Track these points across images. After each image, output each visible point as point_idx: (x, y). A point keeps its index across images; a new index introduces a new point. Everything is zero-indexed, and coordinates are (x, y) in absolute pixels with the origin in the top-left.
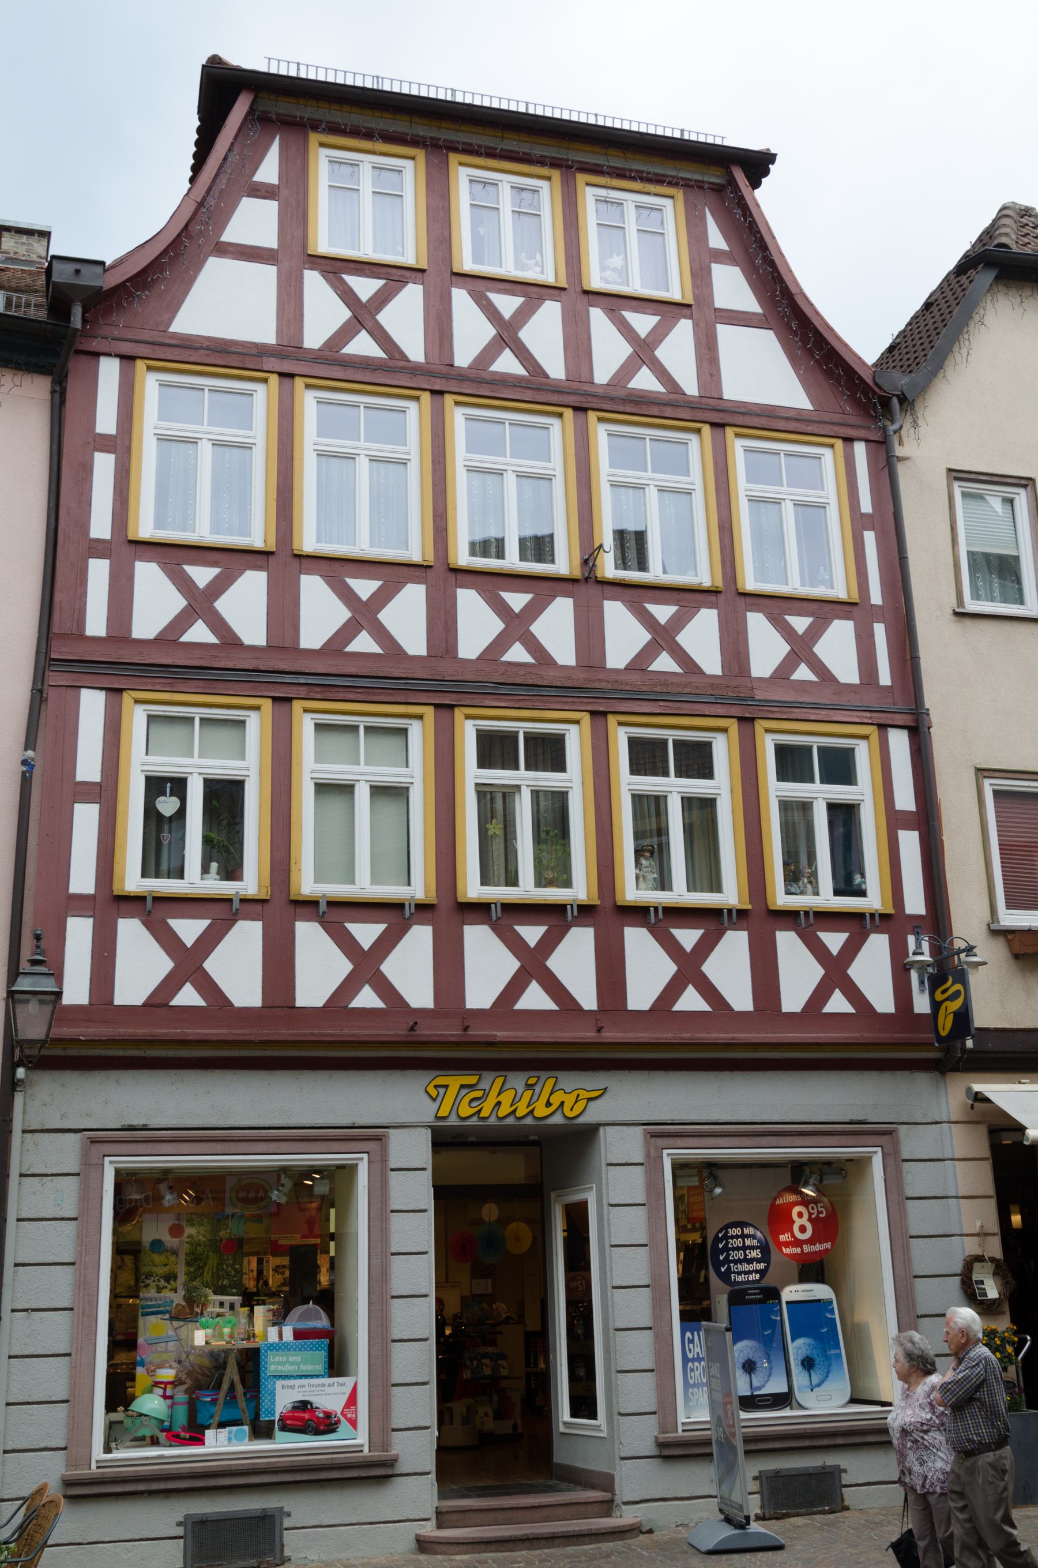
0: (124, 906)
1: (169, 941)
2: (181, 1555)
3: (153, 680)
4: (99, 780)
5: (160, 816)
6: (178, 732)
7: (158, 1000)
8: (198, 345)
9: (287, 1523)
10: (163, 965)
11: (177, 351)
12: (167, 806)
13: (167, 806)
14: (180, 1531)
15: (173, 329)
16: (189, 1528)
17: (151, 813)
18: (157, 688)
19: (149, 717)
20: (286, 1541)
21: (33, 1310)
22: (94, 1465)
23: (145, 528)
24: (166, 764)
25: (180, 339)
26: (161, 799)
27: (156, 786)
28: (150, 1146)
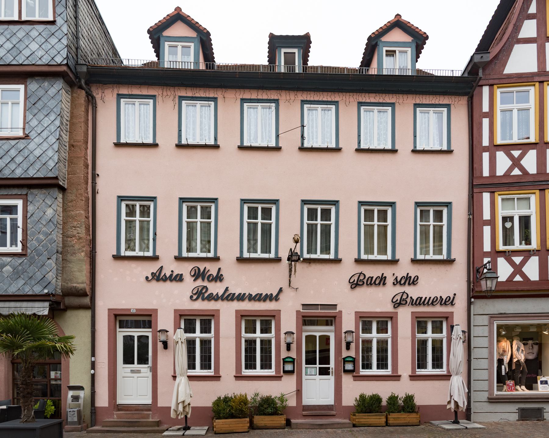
0: (499, 254)
1: (512, 263)
2: (518, 416)
3: (503, 188)
4: (490, 219)
5: (506, 228)
6: (510, 203)
7: (510, 280)
8: (513, 77)
9: (545, 411)
10: (511, 270)
11: (507, 80)
12: (508, 225)
13: (508, 225)
14: (517, 411)
15: (504, 73)
16: (520, 411)
17: (504, 228)
18: (505, 190)
19: (502, 199)
20: (544, 415)
21: (478, 358)
22: (495, 395)
23: (499, 141)
24: (508, 213)
25: (507, 76)
26: (506, 223)
27: (505, 219)
28: (506, 318)
